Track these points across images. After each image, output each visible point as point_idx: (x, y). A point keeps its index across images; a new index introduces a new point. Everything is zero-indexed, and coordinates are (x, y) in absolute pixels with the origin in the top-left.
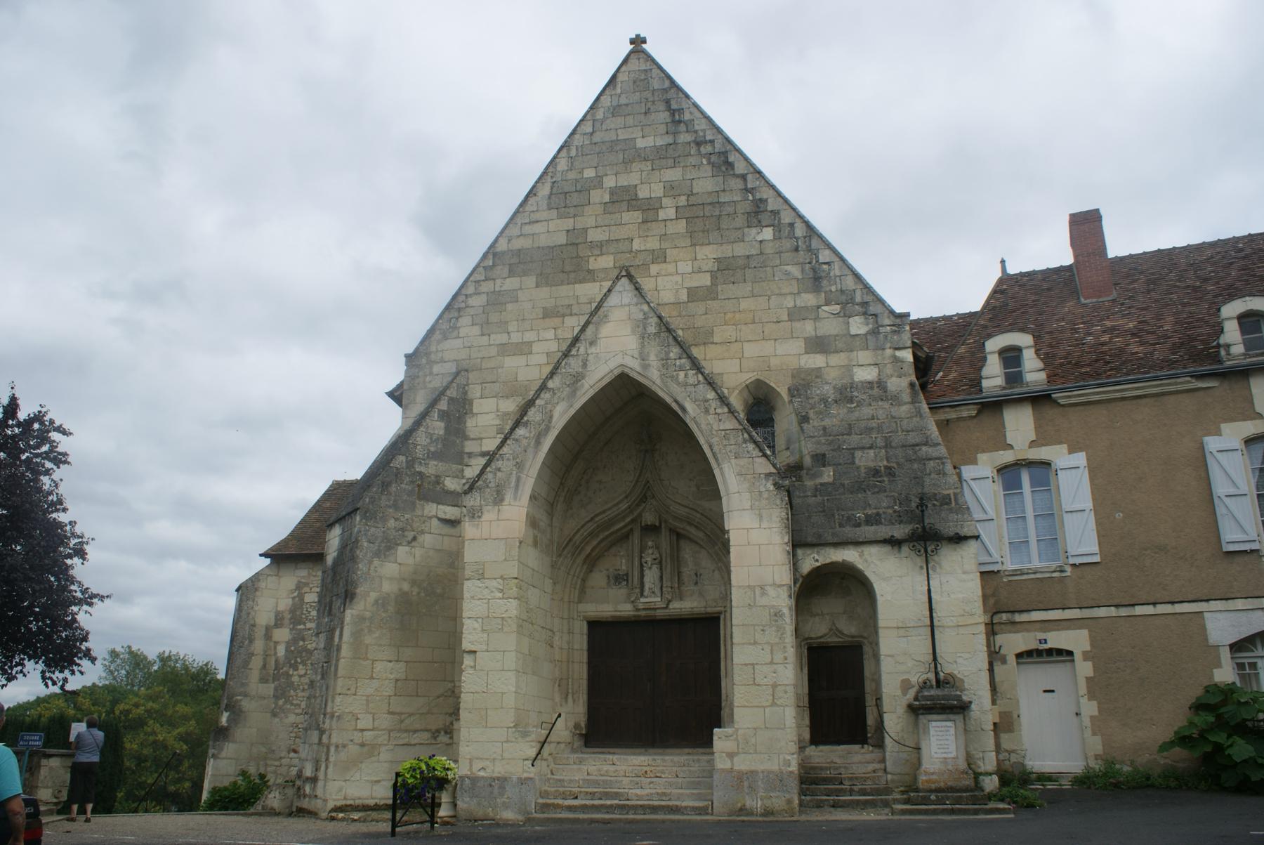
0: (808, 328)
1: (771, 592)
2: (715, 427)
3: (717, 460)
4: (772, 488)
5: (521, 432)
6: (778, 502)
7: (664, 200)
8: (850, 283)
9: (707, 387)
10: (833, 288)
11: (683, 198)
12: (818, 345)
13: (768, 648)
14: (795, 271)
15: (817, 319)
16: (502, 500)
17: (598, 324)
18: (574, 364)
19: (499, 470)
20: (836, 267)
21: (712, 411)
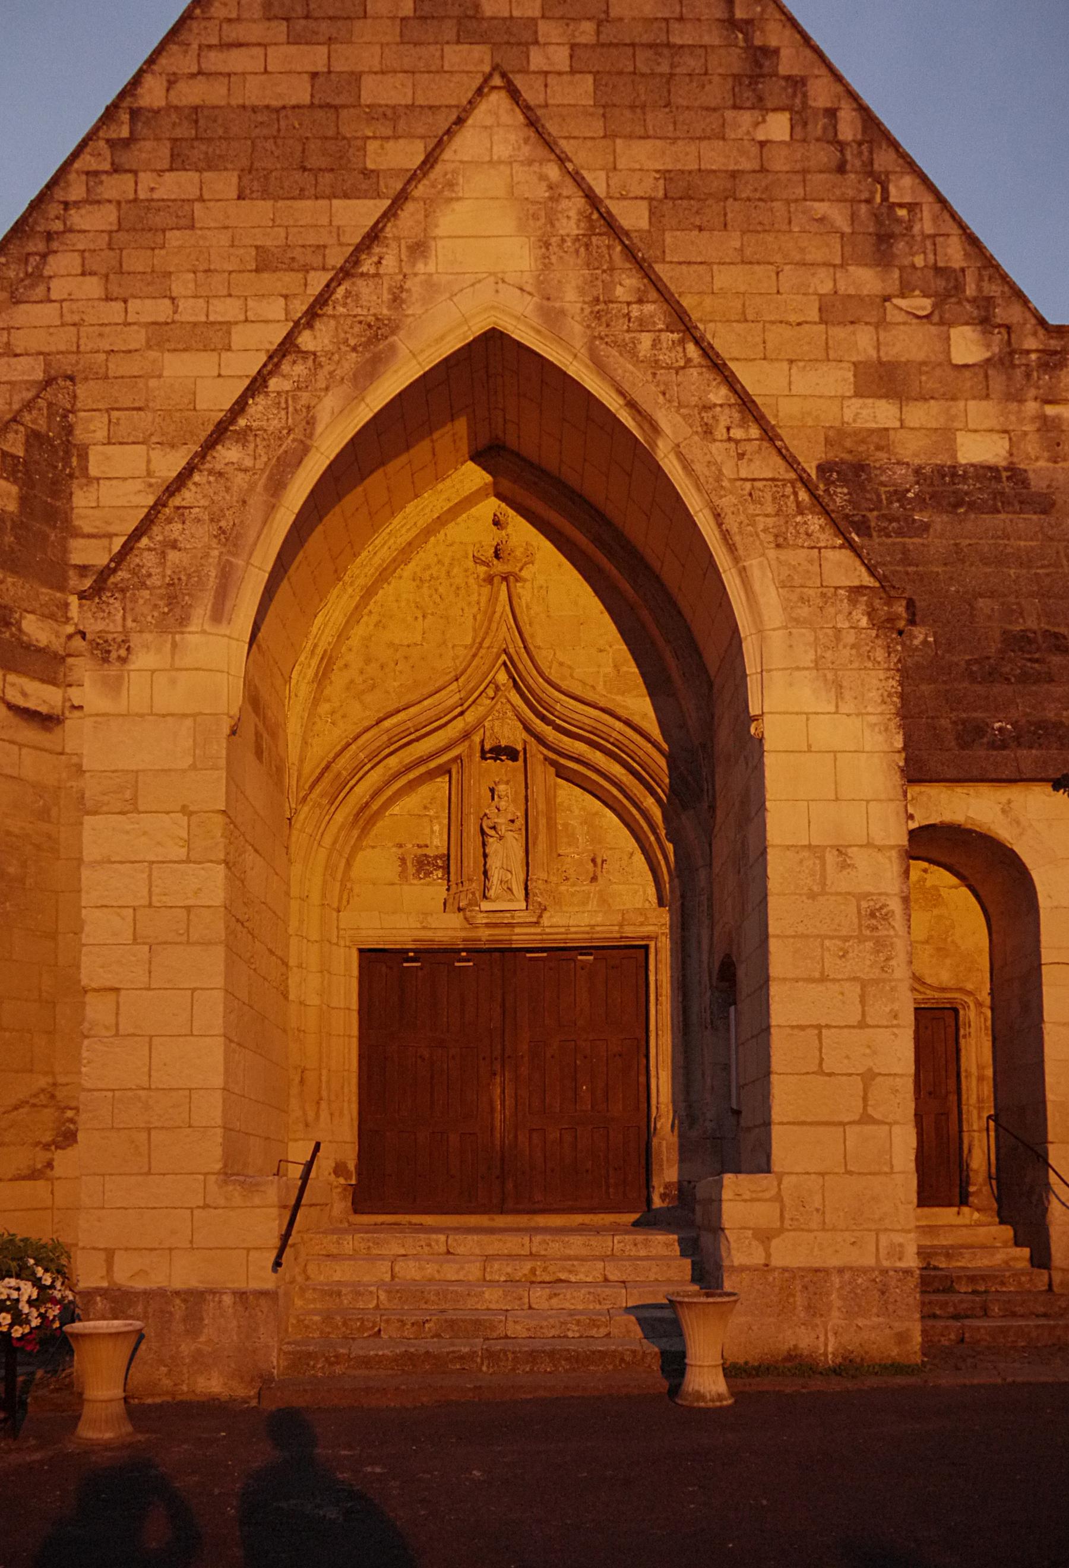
0: (863, 342)
1: (860, 858)
2: (728, 471)
3: (732, 548)
4: (864, 622)
5: (229, 454)
6: (880, 654)
7: (543, 27)
8: (954, 253)
9: (708, 375)
10: (919, 261)
11: (589, 27)
12: (883, 379)
13: (853, 991)
14: (839, 216)
15: (881, 324)
16: (183, 621)
17: (430, 205)
18: (370, 297)
19: (174, 545)
20: (926, 214)
21: (720, 433)
